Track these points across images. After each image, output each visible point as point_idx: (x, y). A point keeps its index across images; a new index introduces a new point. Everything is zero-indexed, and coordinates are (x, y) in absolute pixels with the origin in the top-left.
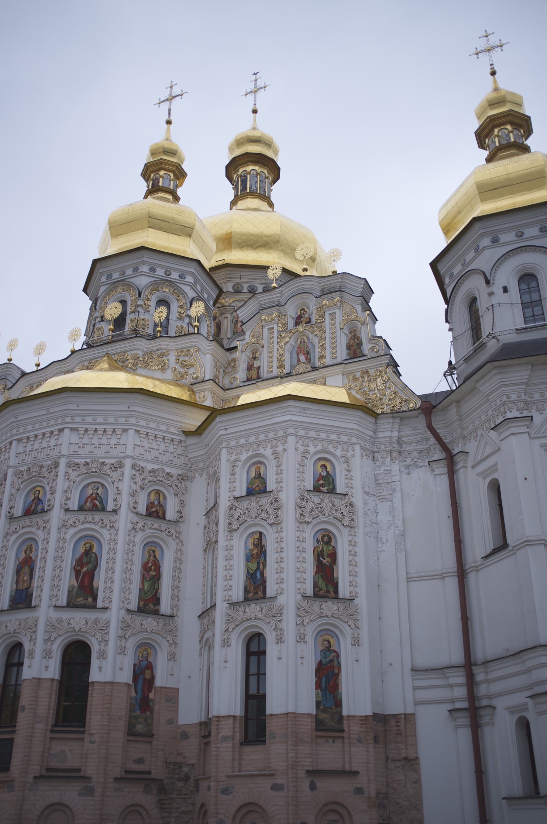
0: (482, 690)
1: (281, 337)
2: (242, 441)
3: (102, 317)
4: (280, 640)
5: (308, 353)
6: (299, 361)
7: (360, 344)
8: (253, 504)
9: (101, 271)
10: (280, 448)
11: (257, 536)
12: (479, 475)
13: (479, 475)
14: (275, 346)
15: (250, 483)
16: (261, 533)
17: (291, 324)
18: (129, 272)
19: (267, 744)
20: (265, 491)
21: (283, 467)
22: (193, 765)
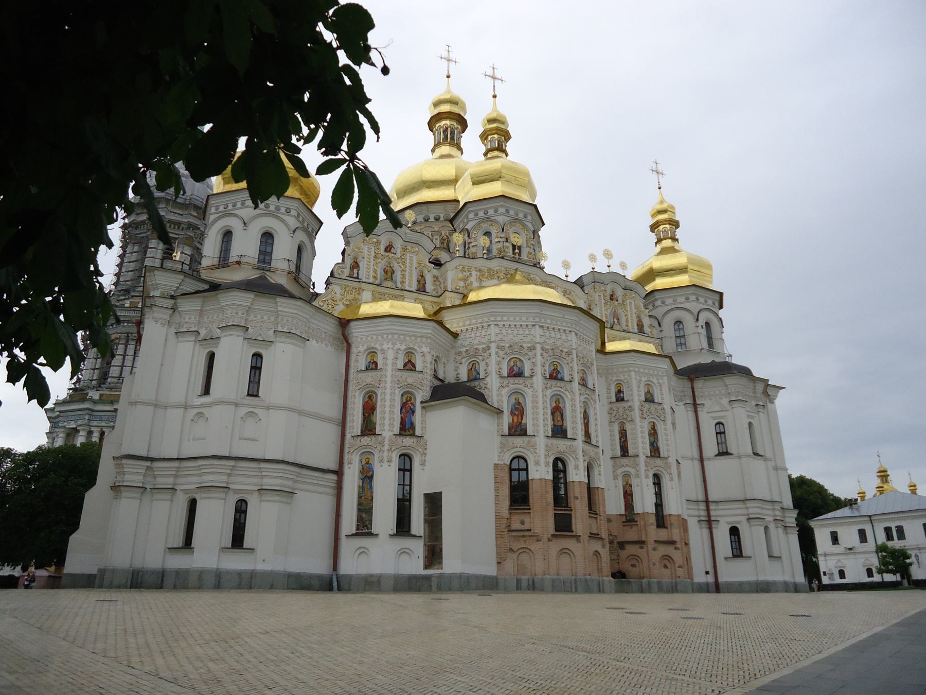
0: (712, 513)
1: (605, 303)
2: (641, 370)
3: (507, 239)
4: (671, 479)
5: (618, 319)
6: (614, 322)
7: (643, 326)
8: (653, 407)
9: (503, 204)
10: (661, 381)
11: (652, 424)
12: (712, 417)
13: (712, 417)
14: (603, 308)
15: (646, 394)
16: (654, 423)
17: (608, 298)
18: (521, 216)
19: (669, 527)
20: (652, 401)
21: (664, 391)
22: (616, 536)
